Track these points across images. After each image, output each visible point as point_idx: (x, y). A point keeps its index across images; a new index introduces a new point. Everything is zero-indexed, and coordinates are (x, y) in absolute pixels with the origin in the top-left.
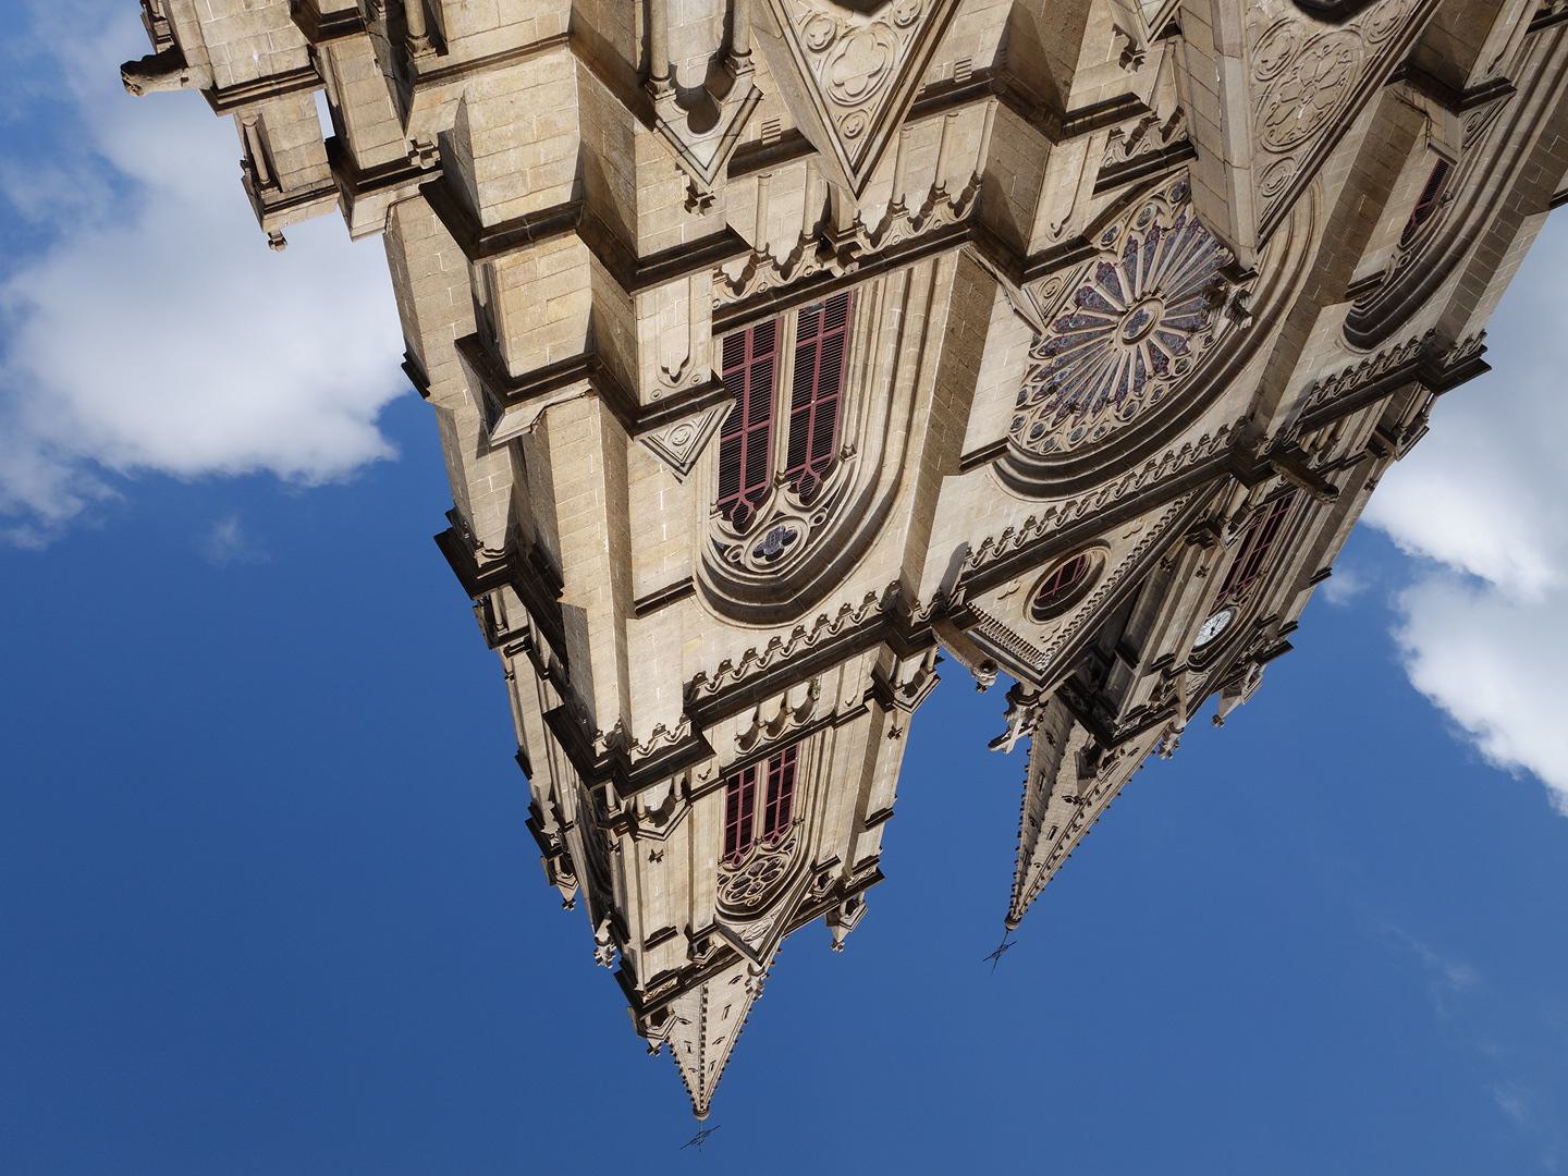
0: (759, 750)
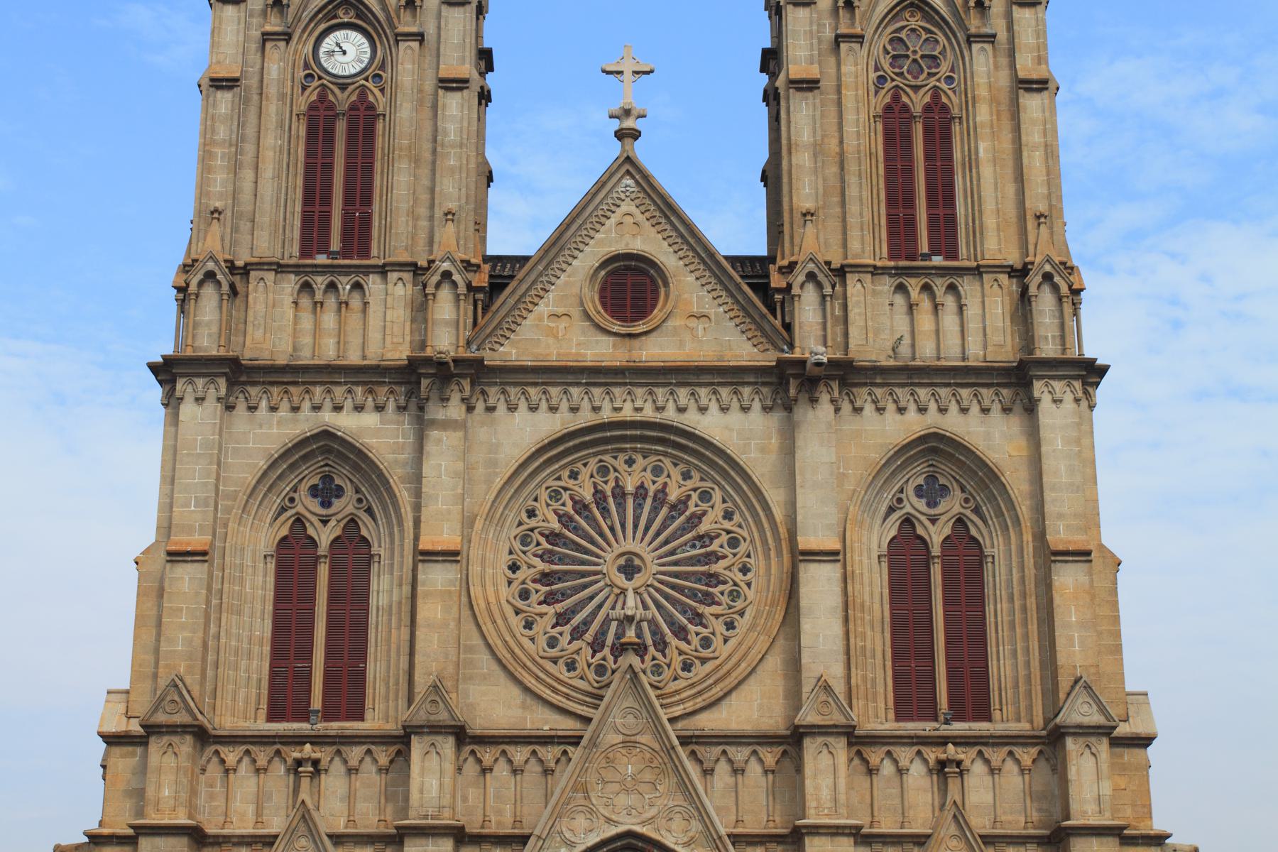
0: (943, 276)
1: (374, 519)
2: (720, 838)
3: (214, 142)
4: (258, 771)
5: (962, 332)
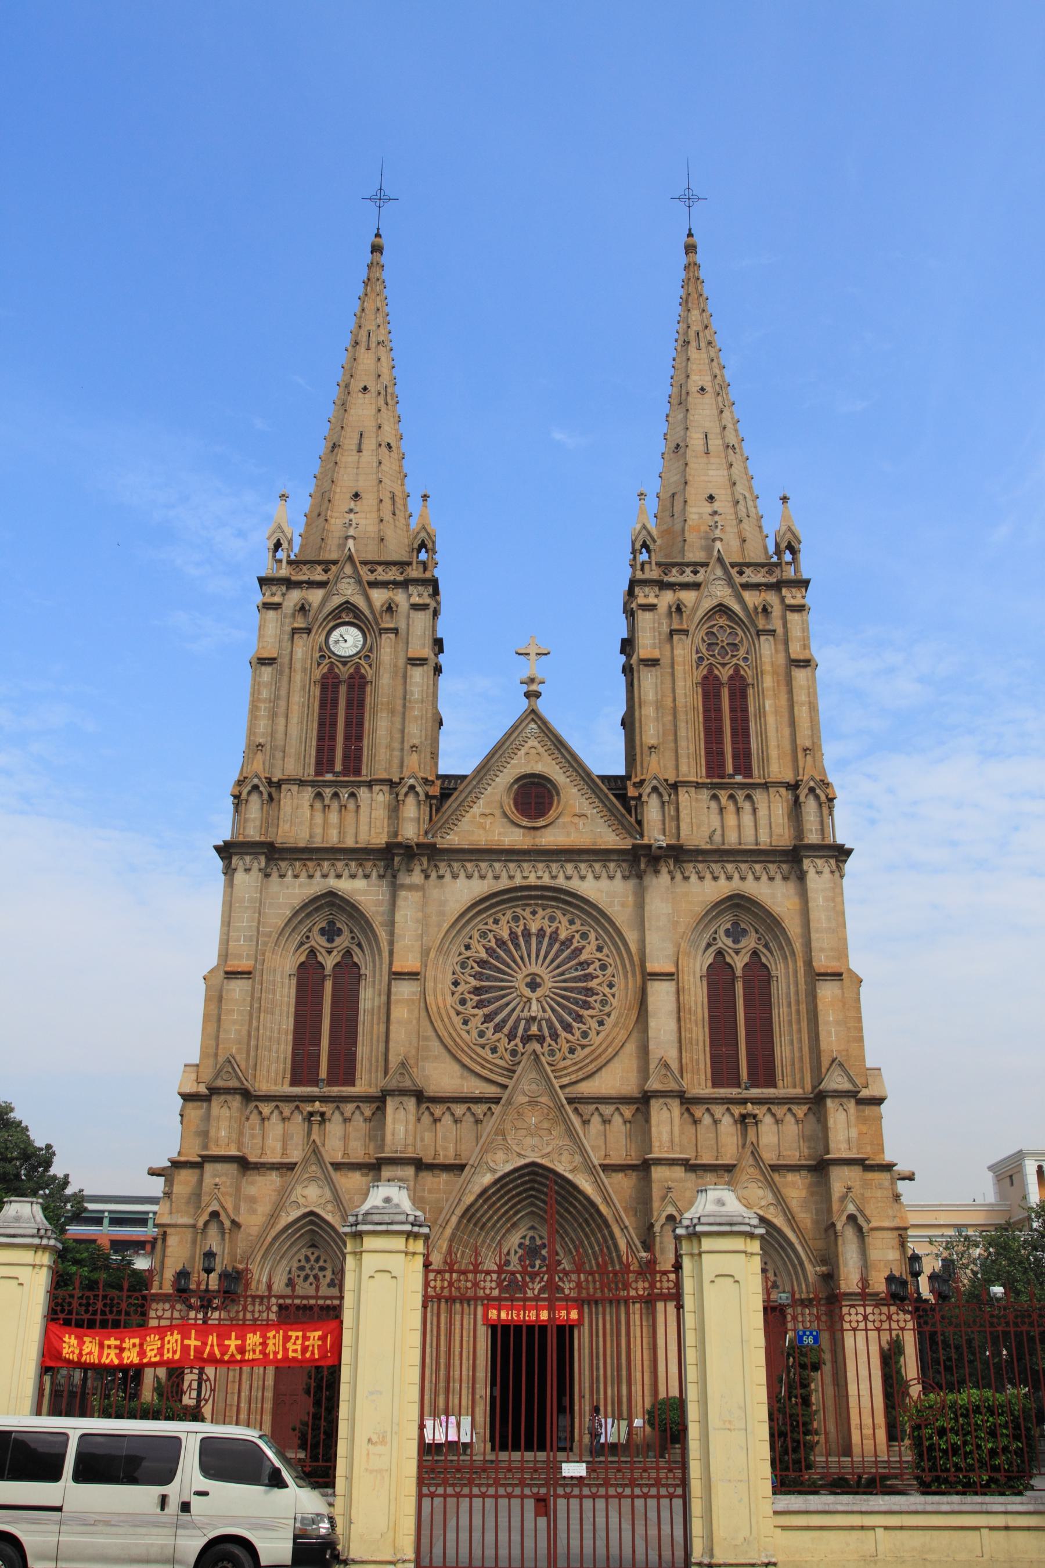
0: (742, 789)
1: (363, 951)
2: (594, 1167)
3: (259, 700)
4: (284, 1119)
5: (756, 826)
